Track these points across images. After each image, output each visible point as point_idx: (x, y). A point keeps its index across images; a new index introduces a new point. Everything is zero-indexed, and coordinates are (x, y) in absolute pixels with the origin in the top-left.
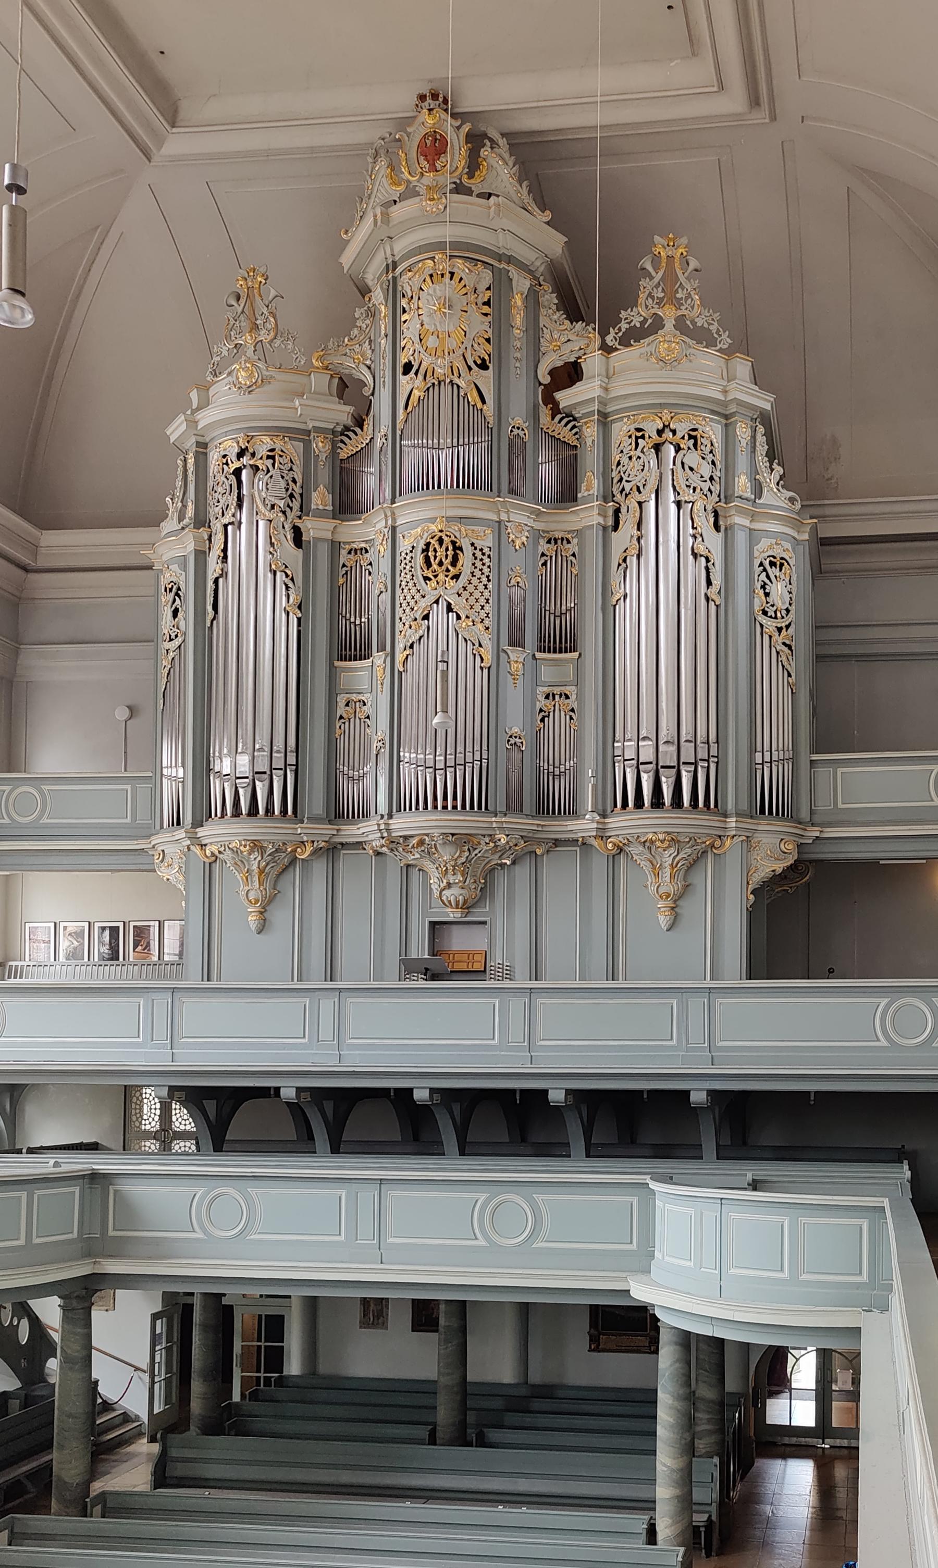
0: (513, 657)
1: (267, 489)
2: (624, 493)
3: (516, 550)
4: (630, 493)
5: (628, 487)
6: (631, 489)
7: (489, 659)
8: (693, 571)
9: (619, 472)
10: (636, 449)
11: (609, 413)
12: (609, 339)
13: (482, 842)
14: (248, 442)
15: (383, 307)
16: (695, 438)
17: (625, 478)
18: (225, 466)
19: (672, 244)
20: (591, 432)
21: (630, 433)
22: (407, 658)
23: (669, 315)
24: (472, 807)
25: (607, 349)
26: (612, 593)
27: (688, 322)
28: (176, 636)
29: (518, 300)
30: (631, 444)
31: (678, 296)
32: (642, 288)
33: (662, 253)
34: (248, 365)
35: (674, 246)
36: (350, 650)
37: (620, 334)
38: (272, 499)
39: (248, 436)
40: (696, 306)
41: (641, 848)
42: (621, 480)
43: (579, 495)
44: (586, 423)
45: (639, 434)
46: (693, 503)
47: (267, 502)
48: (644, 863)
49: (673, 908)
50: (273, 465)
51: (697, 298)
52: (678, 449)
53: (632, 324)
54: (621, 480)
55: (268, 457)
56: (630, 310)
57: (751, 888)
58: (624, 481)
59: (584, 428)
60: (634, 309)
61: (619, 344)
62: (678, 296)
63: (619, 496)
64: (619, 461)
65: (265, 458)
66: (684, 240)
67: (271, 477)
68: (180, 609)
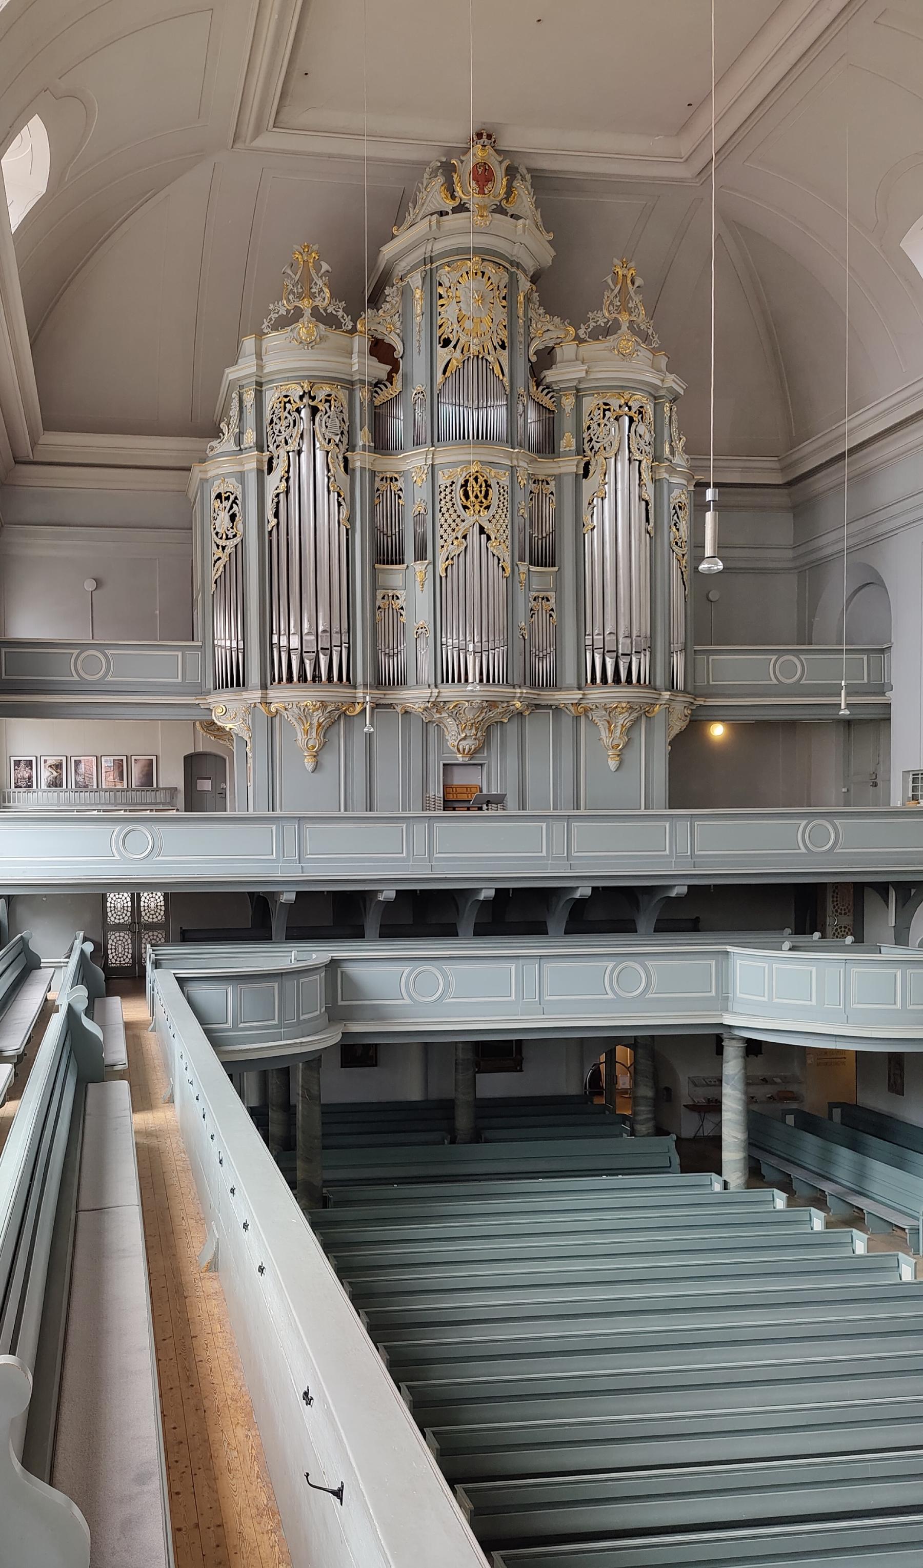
0: (521, 570)
1: (327, 427)
2: (593, 450)
3: (521, 489)
4: (598, 451)
5: (597, 446)
6: (599, 448)
7: (508, 572)
8: (638, 509)
9: (590, 434)
10: (603, 418)
11: (580, 389)
12: (581, 332)
13: (500, 707)
14: (311, 388)
15: (418, 291)
16: (640, 412)
17: (594, 439)
18: (288, 405)
19: (625, 266)
20: (568, 403)
21: (599, 406)
22: (446, 569)
23: (624, 319)
24: (488, 680)
25: (580, 340)
26: (584, 525)
27: (635, 326)
28: (235, 536)
29: (521, 298)
30: (599, 414)
31: (630, 305)
32: (606, 297)
33: (619, 273)
34: (310, 325)
35: (626, 267)
36: (384, 555)
37: (589, 330)
38: (330, 435)
39: (311, 383)
40: (641, 315)
41: (604, 712)
42: (591, 440)
43: (561, 450)
44: (564, 395)
45: (607, 407)
46: (640, 462)
47: (326, 436)
48: (602, 722)
49: (619, 755)
50: (330, 407)
51: (643, 308)
52: (631, 420)
53: (598, 323)
54: (591, 440)
55: (327, 401)
56: (596, 312)
57: (669, 740)
58: (593, 442)
59: (564, 398)
60: (599, 312)
61: (589, 337)
62: (630, 305)
63: (589, 451)
64: (589, 426)
65: (323, 401)
66: (632, 264)
67: (329, 417)
68: (238, 515)
